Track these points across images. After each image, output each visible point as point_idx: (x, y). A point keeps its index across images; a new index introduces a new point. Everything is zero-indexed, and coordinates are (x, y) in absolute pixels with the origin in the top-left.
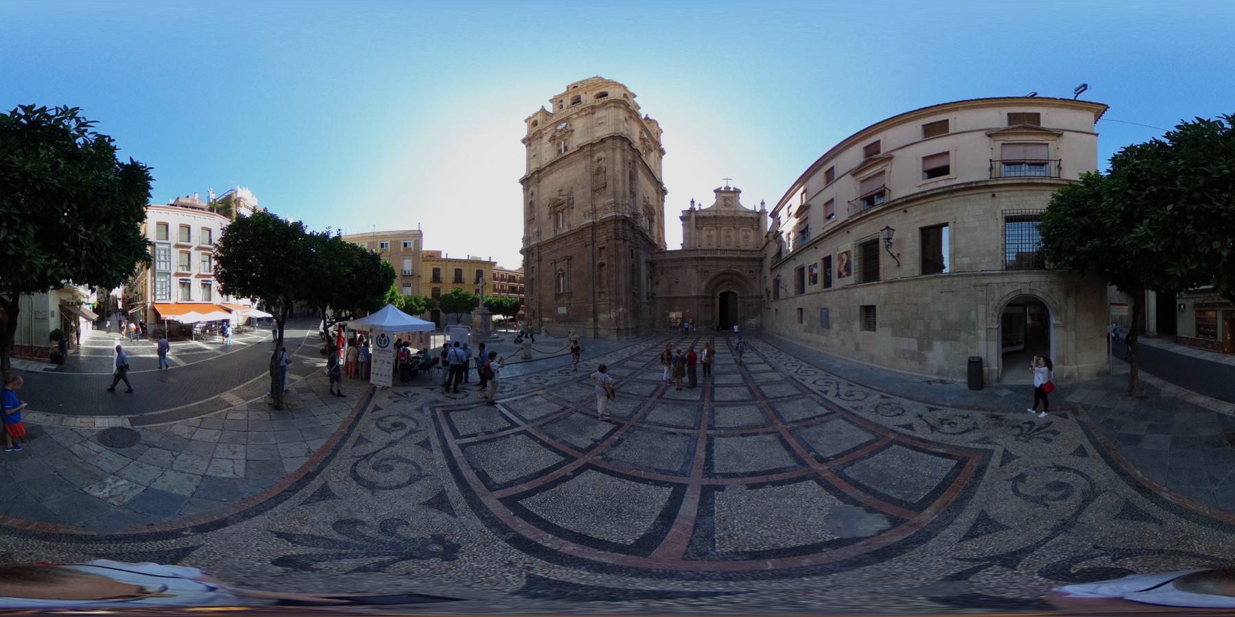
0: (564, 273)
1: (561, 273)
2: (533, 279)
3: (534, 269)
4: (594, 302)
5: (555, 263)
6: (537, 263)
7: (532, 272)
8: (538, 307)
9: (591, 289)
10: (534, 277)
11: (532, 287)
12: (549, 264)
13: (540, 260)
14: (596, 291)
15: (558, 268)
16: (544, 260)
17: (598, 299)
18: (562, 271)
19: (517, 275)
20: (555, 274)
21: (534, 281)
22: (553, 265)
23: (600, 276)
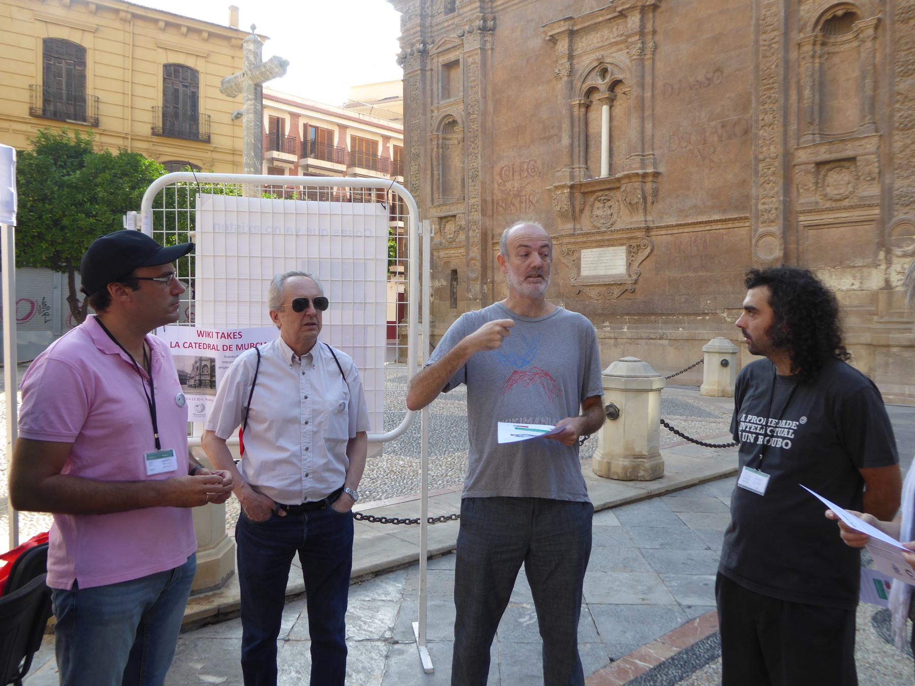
0: (614, 85)
1: (602, 84)
2: (450, 124)
3: (457, 75)
4: (788, 213)
5: (572, 34)
6: (473, 43)
7: (446, 92)
8: (475, 252)
9: (775, 150)
10: (457, 111)
11: (444, 160)
12: (536, 43)
13: (487, 29)
14: (802, 156)
15: (585, 62)
16: (507, 25)
17: (805, 199)
18: (604, 72)
19: (343, 128)
20: (571, 85)
21: (456, 136)
22: (563, 46)
23: (822, 85)
